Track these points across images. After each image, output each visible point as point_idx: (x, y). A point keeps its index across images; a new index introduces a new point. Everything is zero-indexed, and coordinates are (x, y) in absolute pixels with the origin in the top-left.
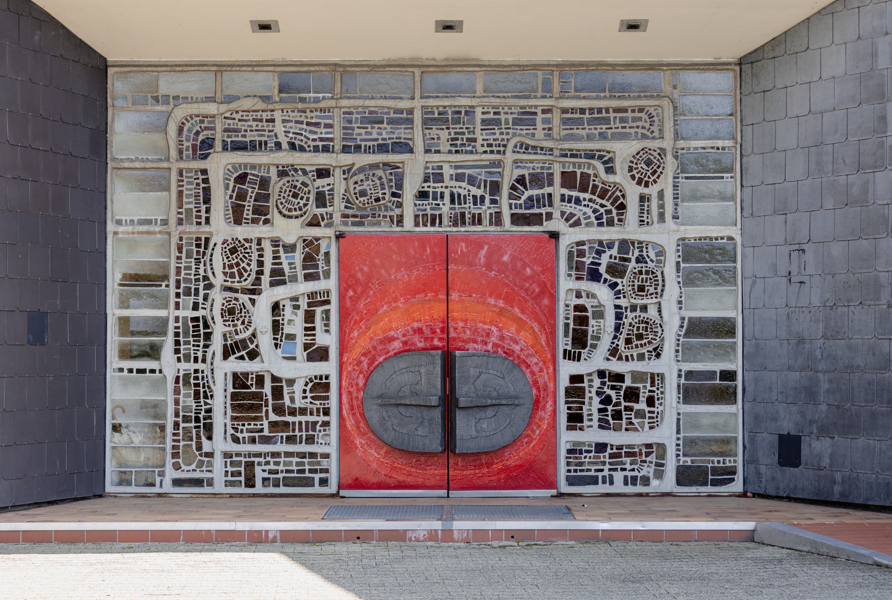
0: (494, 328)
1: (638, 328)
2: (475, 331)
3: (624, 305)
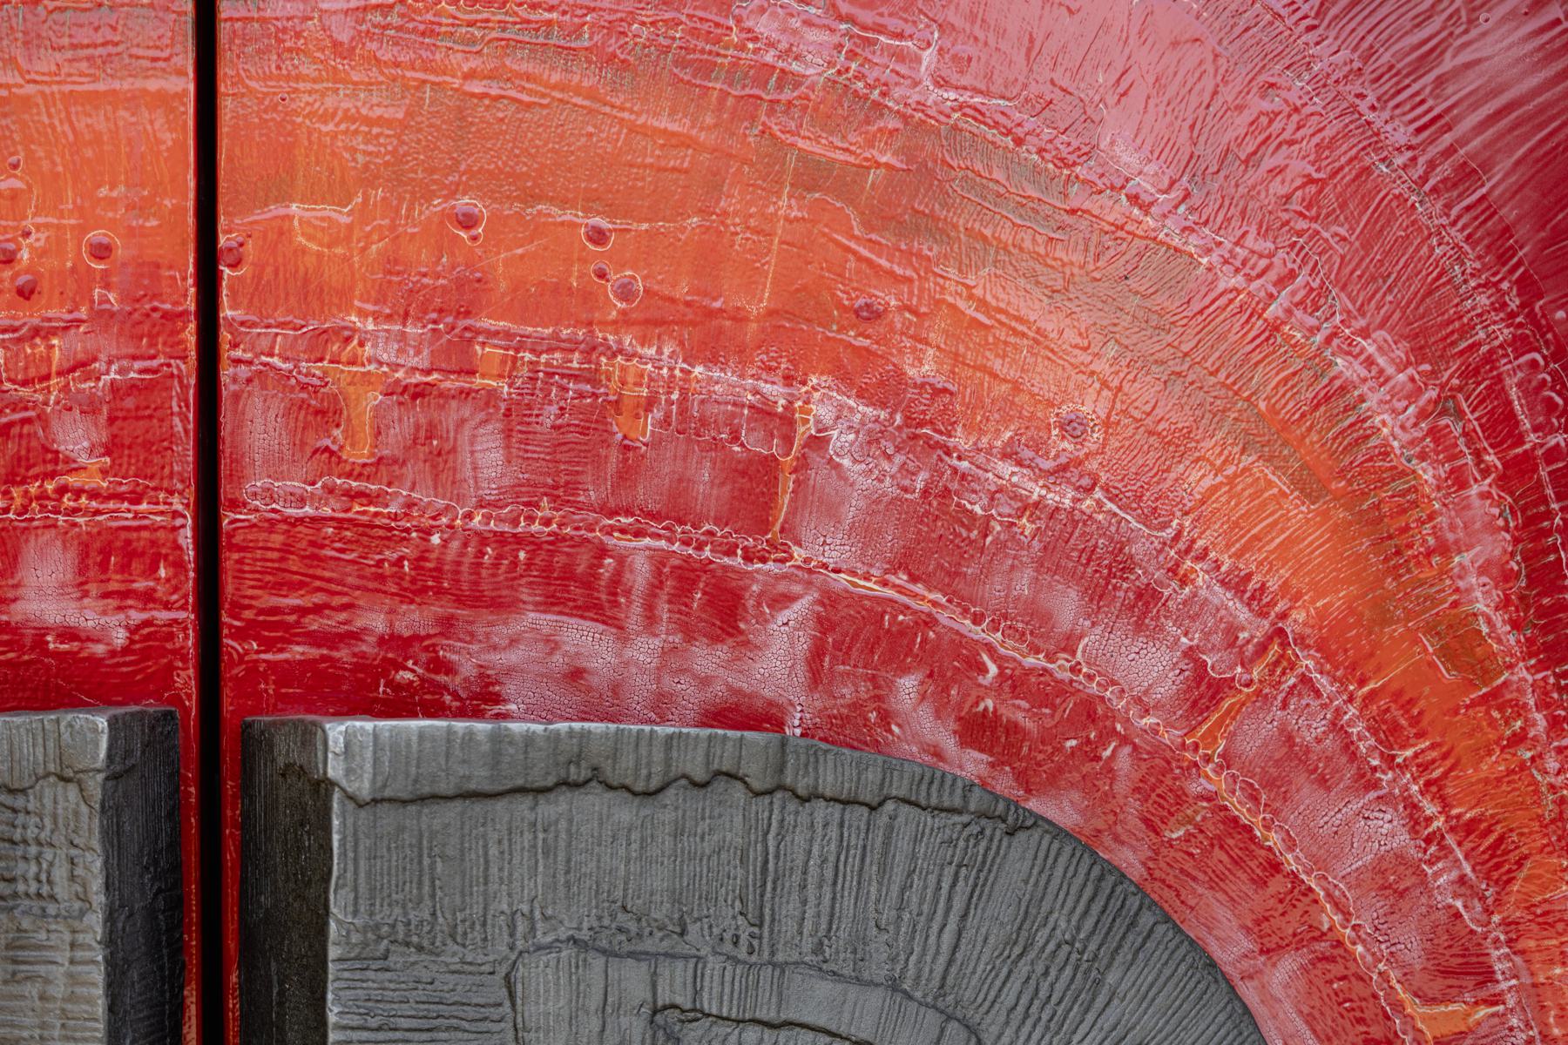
0: (826, 407)
2: (577, 441)
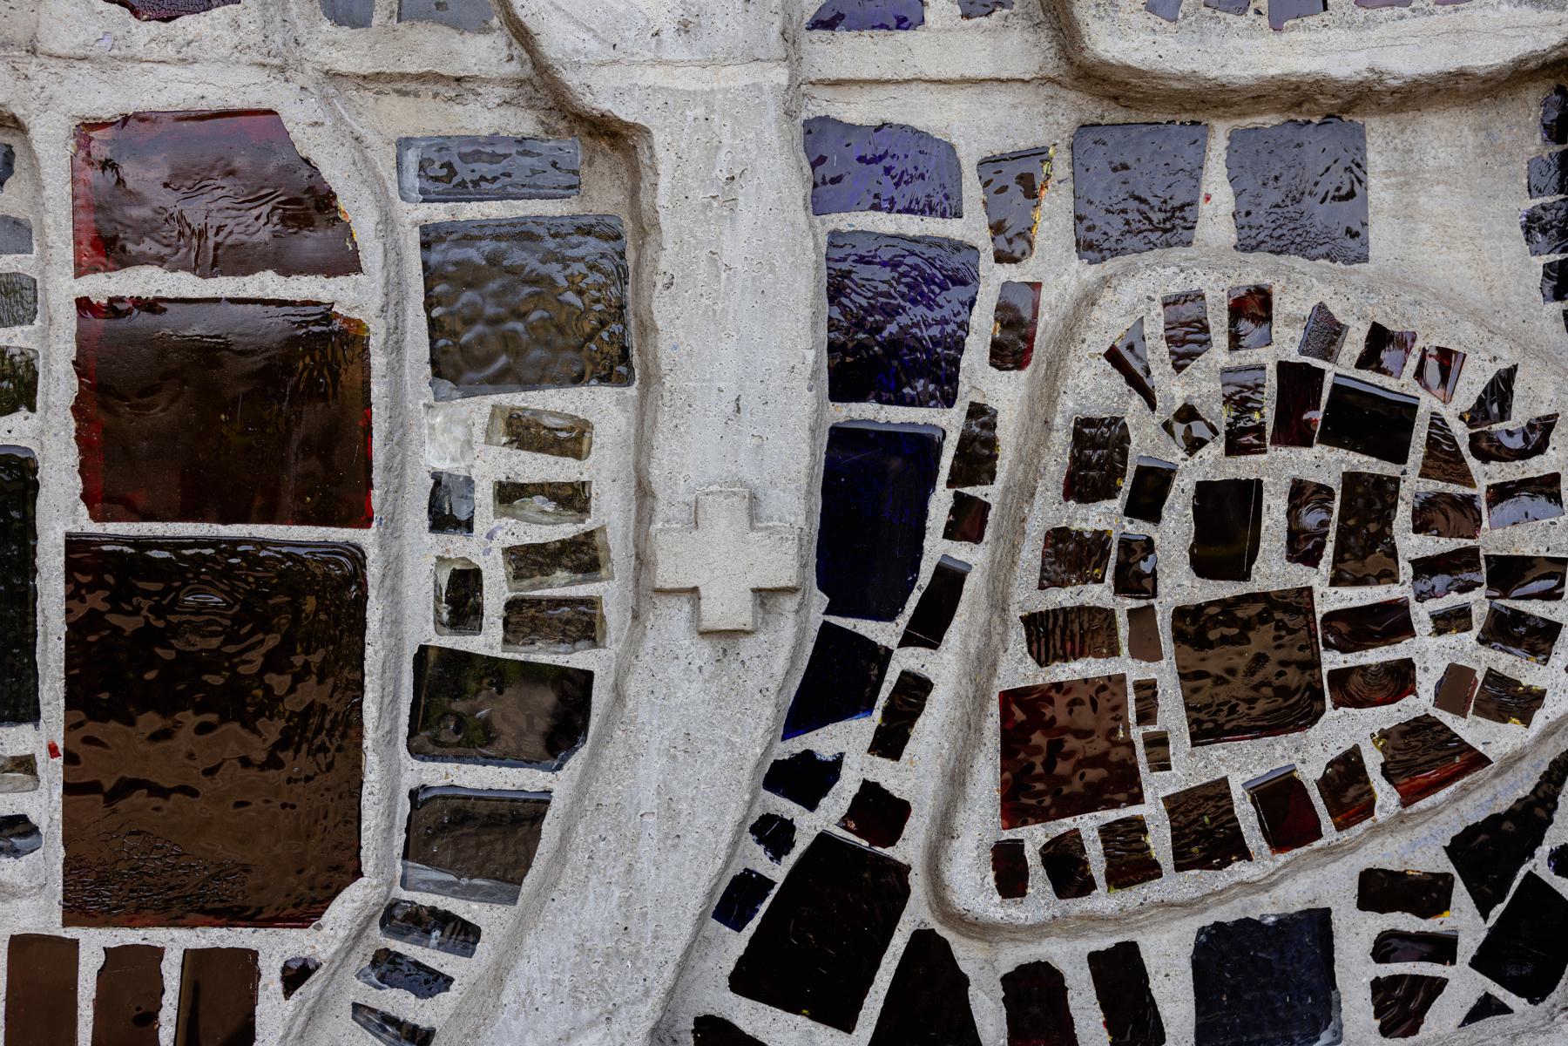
1: (1226, 521)
3: (973, 128)
